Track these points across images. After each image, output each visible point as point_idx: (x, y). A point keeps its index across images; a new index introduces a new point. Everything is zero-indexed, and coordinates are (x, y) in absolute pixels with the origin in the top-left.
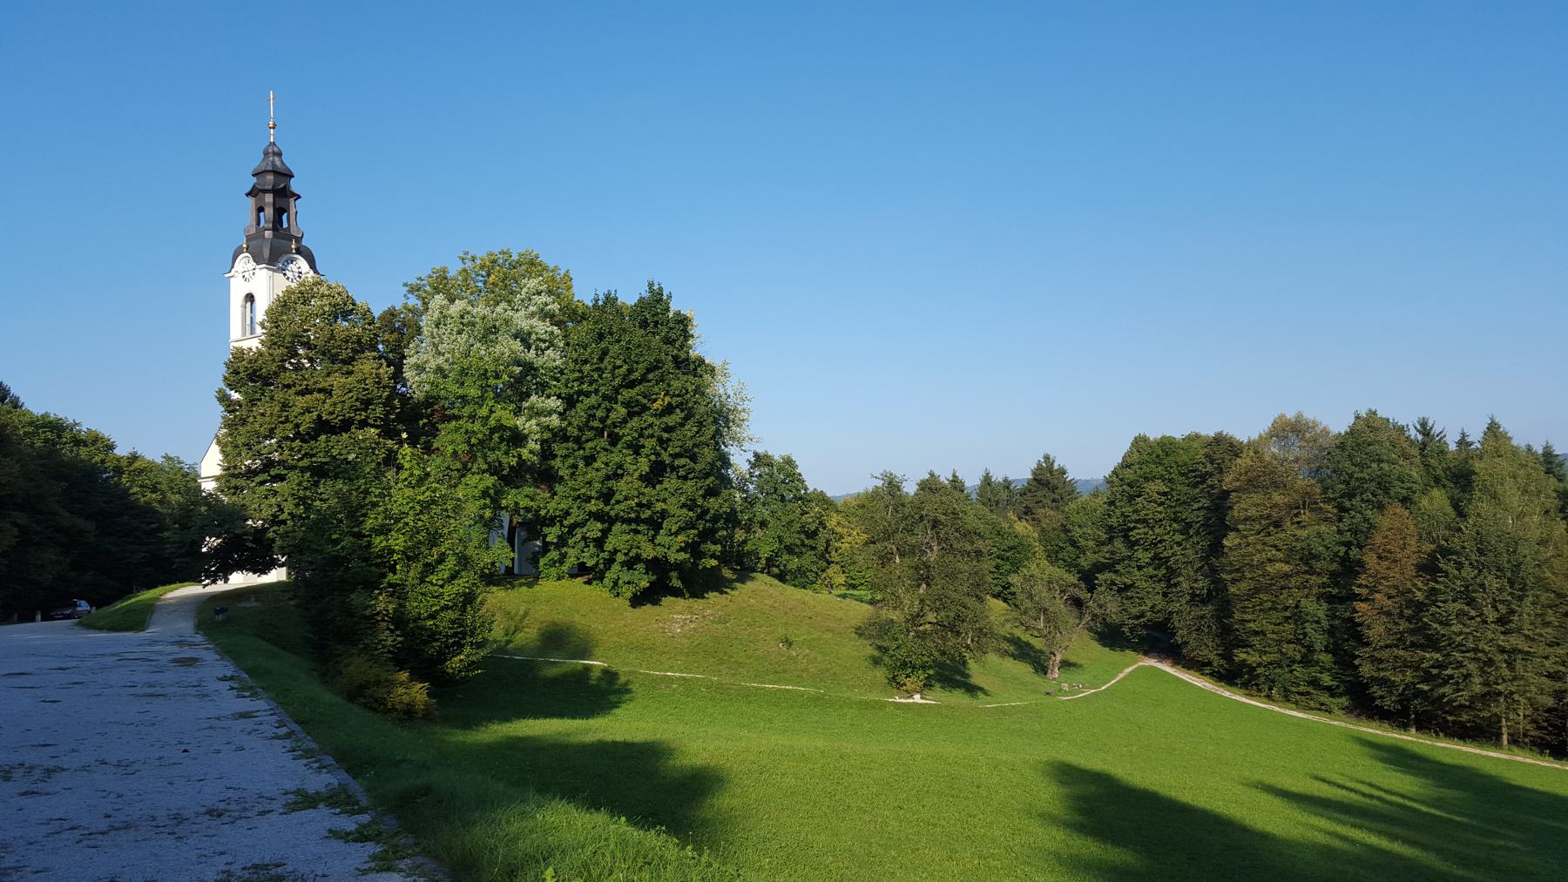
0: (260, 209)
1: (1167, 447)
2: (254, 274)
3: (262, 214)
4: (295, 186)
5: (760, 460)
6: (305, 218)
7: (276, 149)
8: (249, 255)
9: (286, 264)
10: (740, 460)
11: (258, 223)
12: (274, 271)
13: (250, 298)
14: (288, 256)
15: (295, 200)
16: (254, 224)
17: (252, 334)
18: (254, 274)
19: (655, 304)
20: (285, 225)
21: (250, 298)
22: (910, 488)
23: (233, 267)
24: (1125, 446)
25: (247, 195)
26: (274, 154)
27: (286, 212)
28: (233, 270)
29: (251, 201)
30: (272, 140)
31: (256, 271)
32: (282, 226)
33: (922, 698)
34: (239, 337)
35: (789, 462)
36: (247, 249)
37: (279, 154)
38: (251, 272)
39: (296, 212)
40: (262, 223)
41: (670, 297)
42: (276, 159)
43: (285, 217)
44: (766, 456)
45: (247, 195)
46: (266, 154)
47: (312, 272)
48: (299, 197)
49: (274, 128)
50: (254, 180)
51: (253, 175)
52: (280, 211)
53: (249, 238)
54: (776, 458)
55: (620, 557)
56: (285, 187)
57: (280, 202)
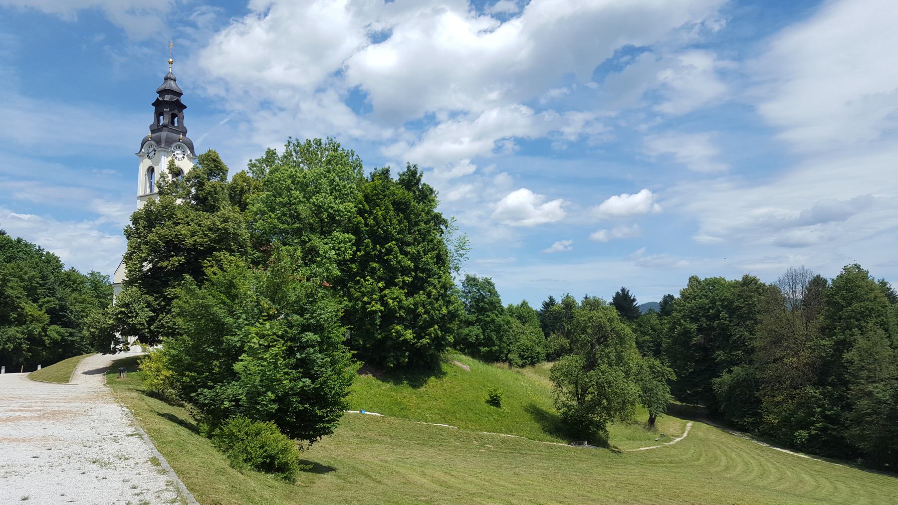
0: (162, 114)
1: (715, 283)
2: (154, 154)
3: (161, 117)
4: (183, 100)
5: (471, 281)
6: (189, 120)
7: (172, 77)
8: (153, 142)
9: (175, 148)
10: (458, 279)
11: (159, 121)
12: (167, 152)
13: (151, 170)
14: (178, 143)
15: (183, 109)
16: (156, 123)
17: (151, 192)
18: (154, 154)
19: (411, 179)
20: (176, 124)
21: (151, 170)
22: (579, 301)
23: (141, 150)
24: (684, 285)
25: (153, 104)
26: (170, 79)
27: (177, 116)
28: (141, 153)
29: (154, 107)
30: (170, 71)
31: (157, 153)
32: (174, 125)
33: (588, 444)
34: (143, 194)
35: (488, 282)
36: (151, 138)
37: (175, 80)
38: (153, 152)
39: (184, 117)
40: (161, 123)
41: (421, 175)
42: (172, 83)
43: (176, 120)
44: (474, 279)
45: (153, 104)
46: (166, 79)
47: (191, 156)
48: (186, 107)
49: (172, 63)
50: (158, 95)
51: (157, 92)
52: (174, 116)
53: (153, 132)
54: (480, 280)
55: (389, 343)
56: (177, 100)
57: (176, 111)
